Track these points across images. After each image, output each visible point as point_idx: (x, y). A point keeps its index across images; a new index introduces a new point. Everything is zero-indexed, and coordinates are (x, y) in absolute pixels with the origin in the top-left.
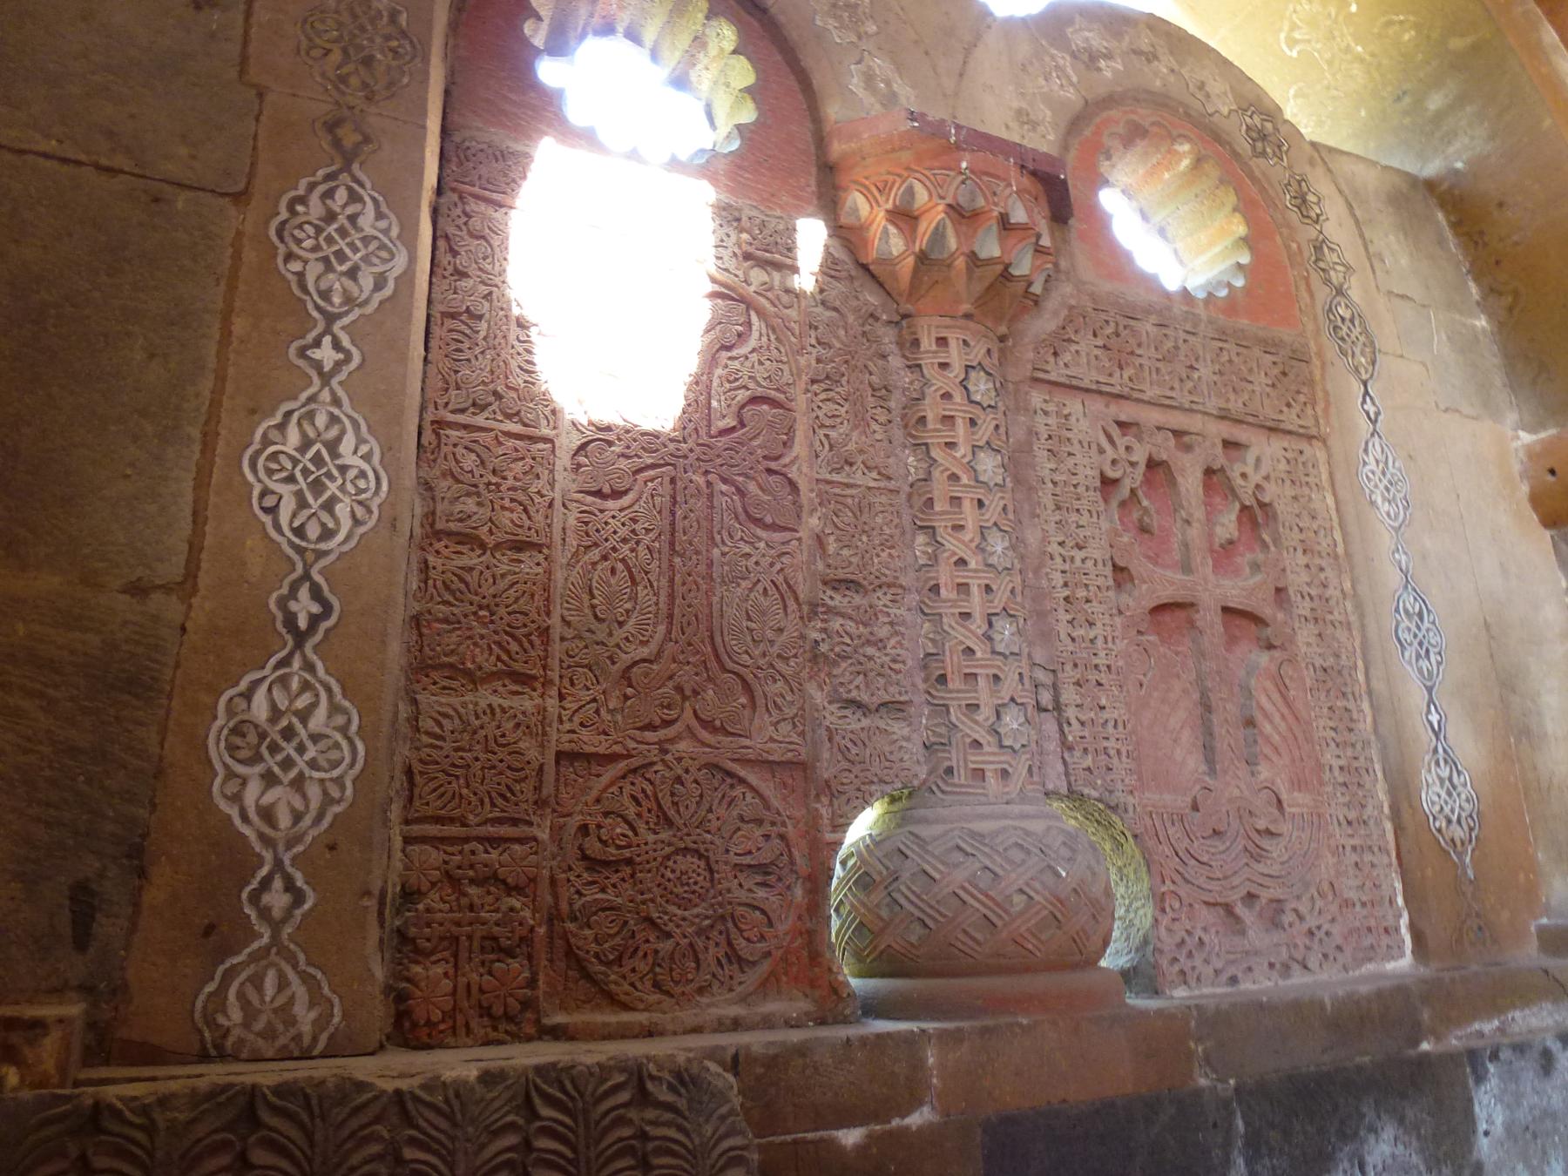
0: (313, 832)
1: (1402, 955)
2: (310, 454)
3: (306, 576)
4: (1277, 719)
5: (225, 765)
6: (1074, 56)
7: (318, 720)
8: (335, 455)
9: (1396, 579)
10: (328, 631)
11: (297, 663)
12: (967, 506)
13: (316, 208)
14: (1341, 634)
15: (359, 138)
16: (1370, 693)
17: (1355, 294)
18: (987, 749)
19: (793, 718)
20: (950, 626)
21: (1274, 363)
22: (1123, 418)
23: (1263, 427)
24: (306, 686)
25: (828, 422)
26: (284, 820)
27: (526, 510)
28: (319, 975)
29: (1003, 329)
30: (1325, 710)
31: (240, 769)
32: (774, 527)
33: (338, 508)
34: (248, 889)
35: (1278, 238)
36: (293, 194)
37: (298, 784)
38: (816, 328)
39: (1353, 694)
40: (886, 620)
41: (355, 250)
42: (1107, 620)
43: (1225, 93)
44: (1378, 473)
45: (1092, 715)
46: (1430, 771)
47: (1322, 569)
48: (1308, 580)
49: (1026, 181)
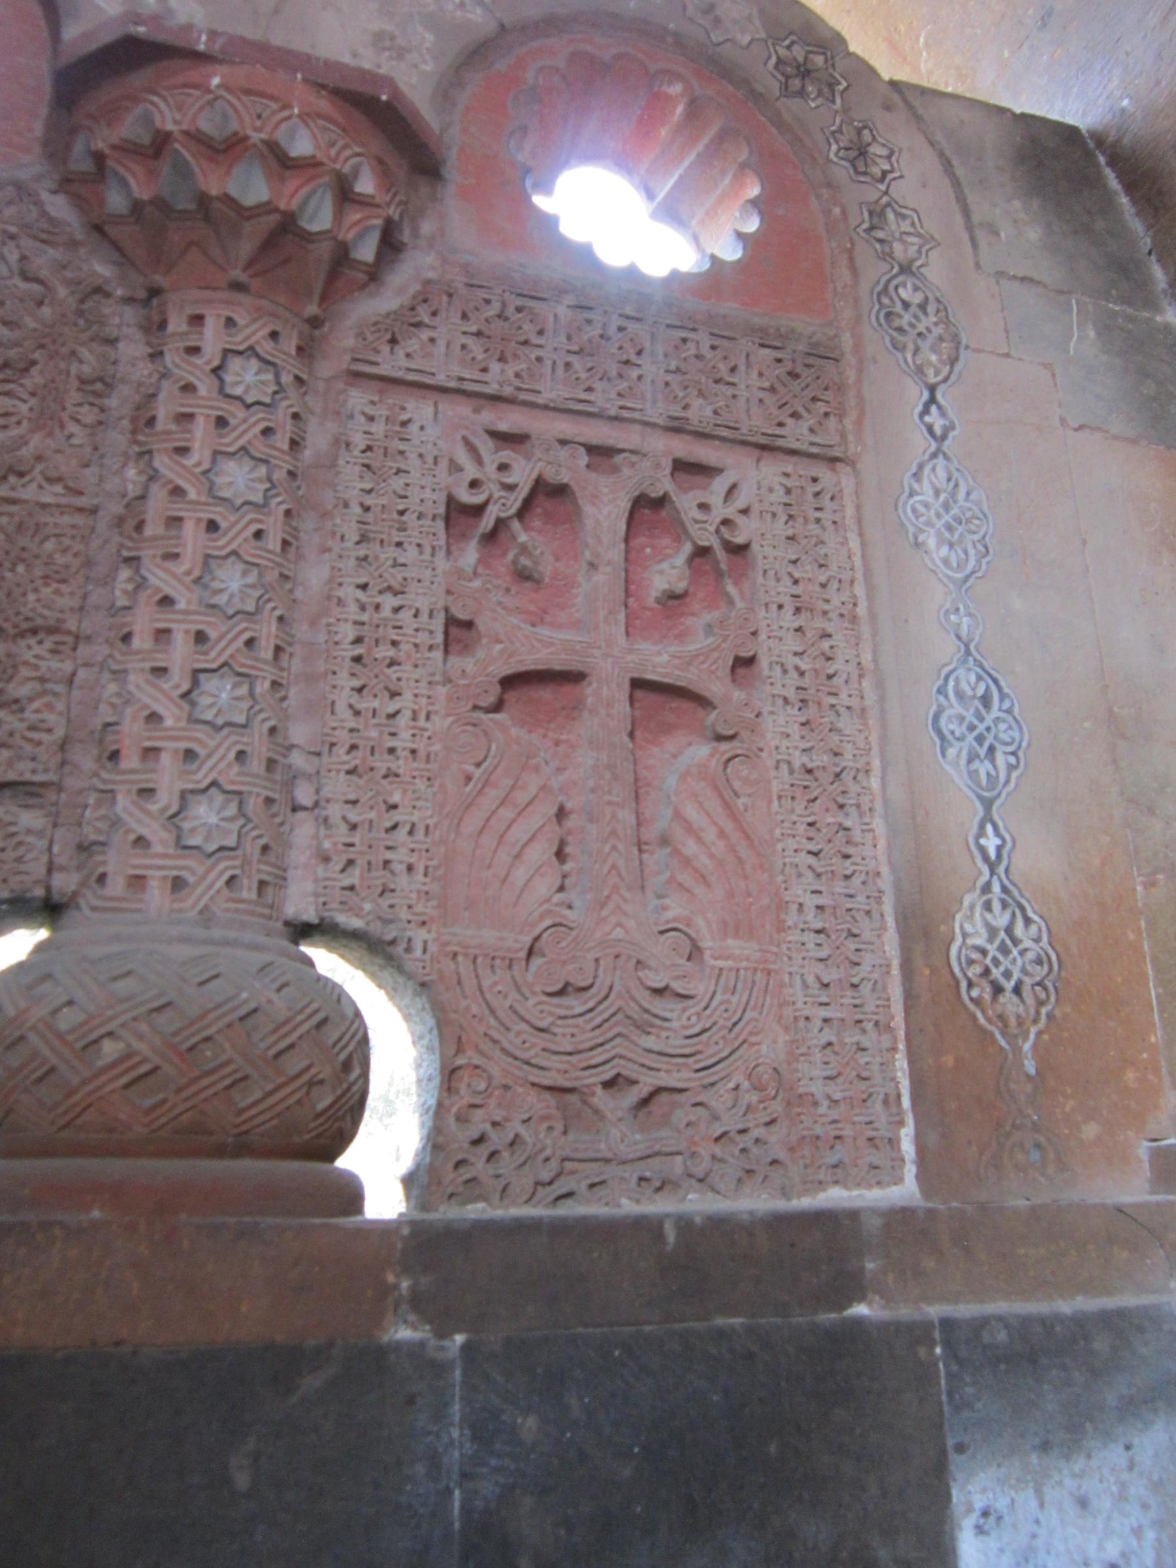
1: (899, 1180)
4: (710, 835)
9: (948, 650)
12: (191, 532)
14: (845, 723)
16: (886, 802)
17: (935, 270)
18: (158, 849)
20: (138, 686)
21: (779, 361)
22: (503, 427)
23: (744, 443)
29: (312, 309)
30: (802, 828)
35: (814, 204)
39: (858, 806)
40: (34, 674)
42: (423, 689)
43: (749, 19)
44: (937, 505)
45: (372, 815)
46: (971, 917)
48: (800, 649)
49: (323, 104)
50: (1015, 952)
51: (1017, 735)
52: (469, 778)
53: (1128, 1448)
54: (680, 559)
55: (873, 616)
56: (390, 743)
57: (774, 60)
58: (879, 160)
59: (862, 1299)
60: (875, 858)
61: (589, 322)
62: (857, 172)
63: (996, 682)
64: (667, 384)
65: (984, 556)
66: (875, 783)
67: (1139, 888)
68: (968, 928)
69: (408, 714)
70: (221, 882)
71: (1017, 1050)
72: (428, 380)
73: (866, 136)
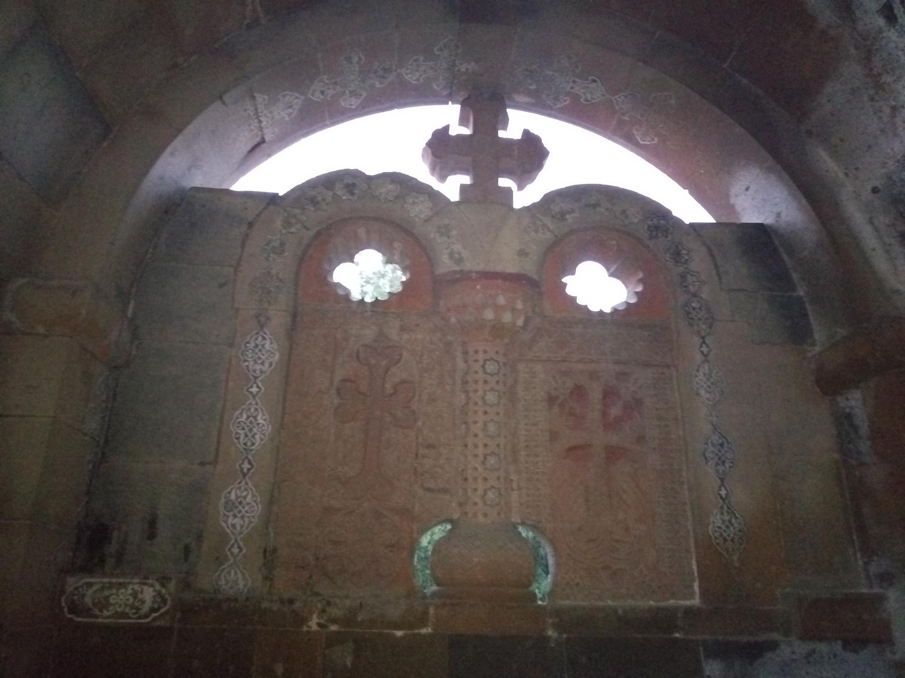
3: (247, 458)
6: (553, 217)
7: (249, 499)
8: (256, 420)
10: (253, 473)
11: (243, 483)
13: (252, 345)
17: (705, 294)
24: (246, 490)
26: (238, 527)
31: (227, 513)
37: (242, 517)
41: (263, 355)
47: (667, 426)
50: (732, 528)
58: (683, 255)
66: (684, 474)
72: (541, 359)
73: (680, 246)
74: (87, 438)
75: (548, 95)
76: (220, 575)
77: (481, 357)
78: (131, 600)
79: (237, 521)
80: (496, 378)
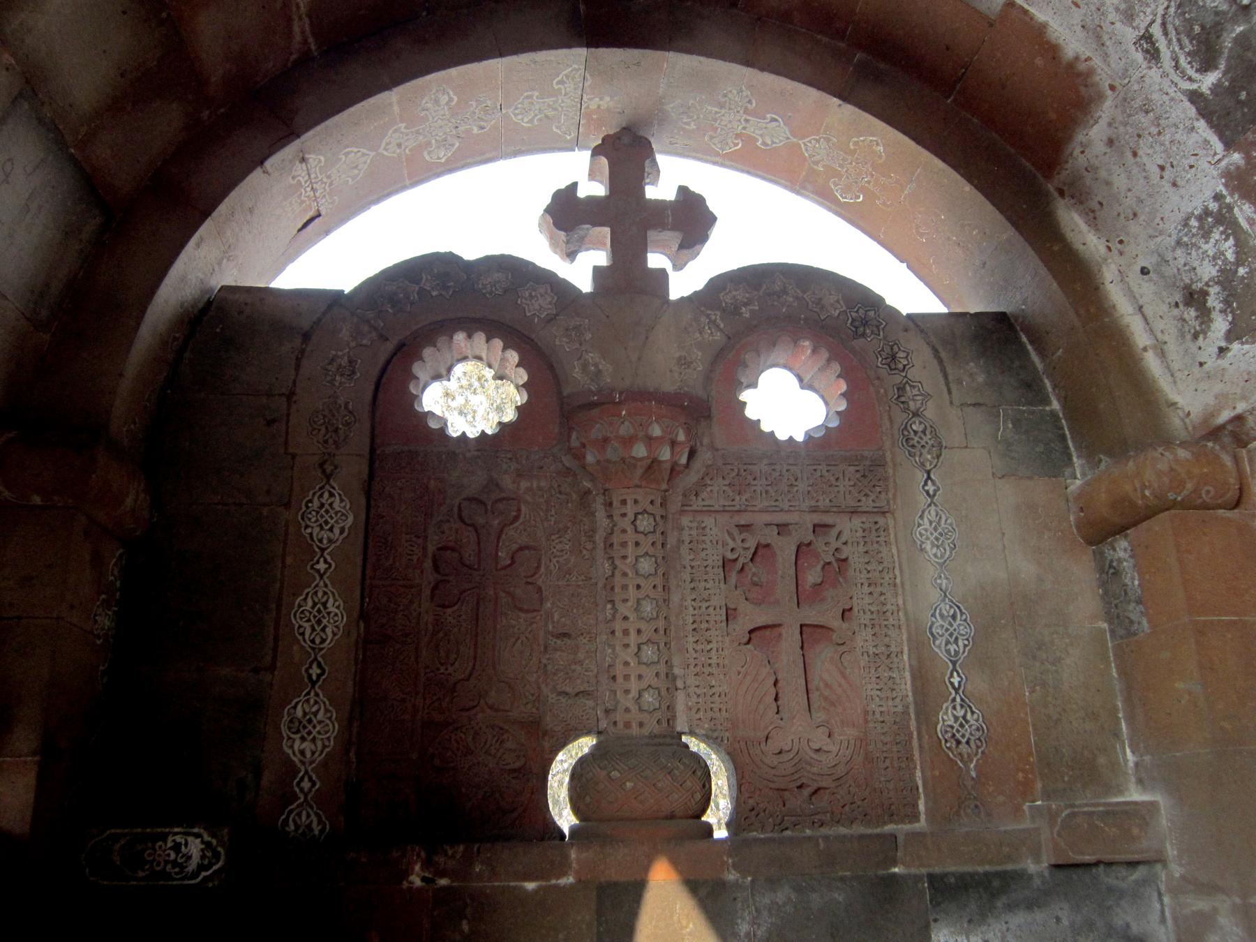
0: (319, 759)
2: (316, 609)
3: (316, 659)
5: (288, 735)
6: (724, 310)
7: (320, 716)
8: (325, 608)
9: (935, 595)
10: (324, 680)
13: (316, 503)
15: (332, 468)
17: (930, 412)
19: (534, 701)
21: (857, 471)
25: (558, 554)
26: (308, 754)
27: (408, 619)
28: (321, 813)
29: (664, 486)
31: (292, 736)
32: (527, 611)
33: (327, 629)
34: (296, 781)
35: (872, 388)
36: (307, 499)
37: (314, 740)
38: (555, 506)
42: (720, 639)
43: (838, 301)
44: (931, 529)
46: (946, 713)
51: (969, 631)
52: (739, 673)
53: (1006, 923)
54: (819, 568)
55: (903, 584)
56: (710, 661)
57: (850, 321)
58: (901, 360)
59: (895, 867)
60: (906, 689)
61: (774, 470)
62: (891, 369)
63: (959, 607)
64: (809, 492)
65: (954, 549)
67: (1027, 694)
68: (945, 717)
69: (715, 649)
70: (655, 722)
71: (968, 770)
72: (712, 509)
74: (99, 642)
75: (711, 138)
76: (286, 822)
77: (630, 509)
78: (173, 856)
79: (307, 746)
80: (651, 538)
